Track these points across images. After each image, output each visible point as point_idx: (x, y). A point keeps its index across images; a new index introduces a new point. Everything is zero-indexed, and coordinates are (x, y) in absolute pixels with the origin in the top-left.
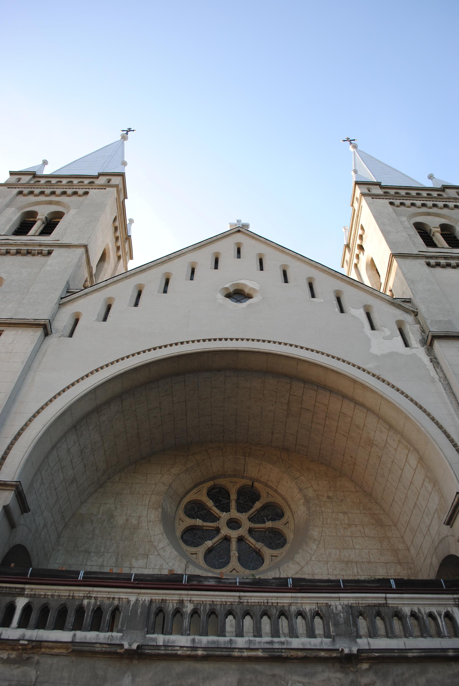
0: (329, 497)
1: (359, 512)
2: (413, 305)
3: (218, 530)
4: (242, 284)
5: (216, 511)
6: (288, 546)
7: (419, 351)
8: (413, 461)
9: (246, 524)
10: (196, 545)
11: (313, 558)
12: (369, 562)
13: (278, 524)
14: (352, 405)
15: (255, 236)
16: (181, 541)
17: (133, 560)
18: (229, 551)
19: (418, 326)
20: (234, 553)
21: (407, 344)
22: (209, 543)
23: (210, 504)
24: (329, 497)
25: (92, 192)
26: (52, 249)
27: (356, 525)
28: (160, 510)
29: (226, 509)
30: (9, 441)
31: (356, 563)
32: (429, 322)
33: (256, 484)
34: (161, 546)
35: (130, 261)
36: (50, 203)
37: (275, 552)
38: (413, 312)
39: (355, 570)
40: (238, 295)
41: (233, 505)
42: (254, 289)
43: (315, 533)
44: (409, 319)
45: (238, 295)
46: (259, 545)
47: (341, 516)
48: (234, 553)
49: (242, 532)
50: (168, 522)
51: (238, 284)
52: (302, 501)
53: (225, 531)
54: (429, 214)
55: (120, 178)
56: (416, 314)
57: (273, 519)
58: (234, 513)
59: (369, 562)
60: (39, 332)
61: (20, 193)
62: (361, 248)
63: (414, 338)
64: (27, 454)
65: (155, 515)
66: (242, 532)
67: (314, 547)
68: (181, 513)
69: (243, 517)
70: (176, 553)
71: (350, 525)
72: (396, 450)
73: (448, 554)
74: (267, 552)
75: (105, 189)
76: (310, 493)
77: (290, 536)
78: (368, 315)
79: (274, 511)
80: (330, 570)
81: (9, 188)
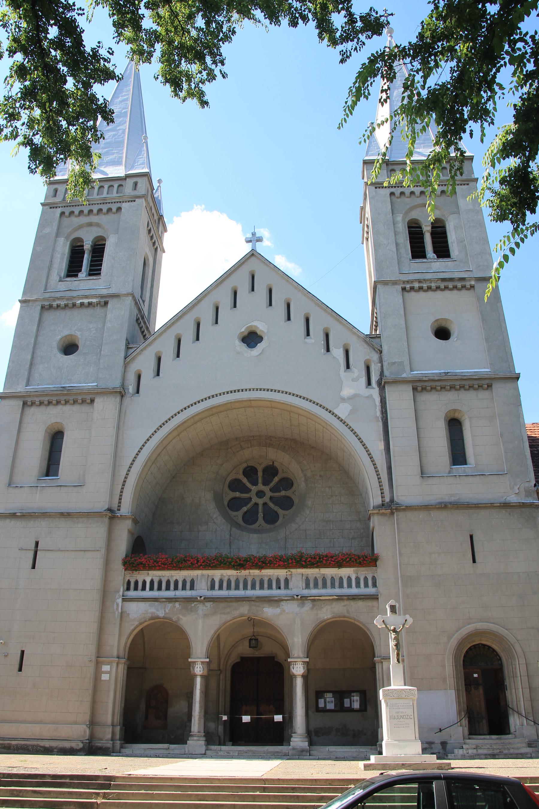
0: (321, 476)
1: (339, 486)
4: (255, 326)
5: (248, 485)
6: (294, 507)
7: (375, 392)
9: (269, 494)
10: (237, 510)
11: (307, 520)
12: (341, 521)
13: (288, 493)
15: (266, 262)
16: (227, 508)
17: (199, 527)
18: (257, 512)
19: (380, 365)
20: (261, 515)
21: (369, 383)
22: (245, 509)
23: (245, 480)
24: (321, 476)
25: (125, 206)
26: (107, 300)
27: (336, 496)
28: (212, 492)
29: (255, 483)
30: (120, 487)
31: (333, 521)
33: (276, 464)
34: (215, 516)
35: (165, 234)
36: (90, 225)
37: (286, 512)
39: (332, 527)
40: (251, 339)
41: (260, 480)
42: (263, 331)
43: (309, 503)
44: (375, 357)
45: (251, 339)
46: (276, 508)
47: (327, 489)
48: (261, 515)
49: (266, 499)
50: (218, 498)
51: (251, 326)
52: (303, 479)
55: (145, 179)
56: (381, 352)
57: (285, 490)
58: (261, 487)
59: (341, 521)
60: (118, 399)
61: (63, 214)
64: (132, 495)
65: (209, 496)
66: (266, 499)
67: (308, 512)
68: (227, 489)
69: (266, 489)
70: (224, 521)
71: (332, 496)
74: (281, 512)
75: (134, 201)
76: (309, 473)
77: (296, 501)
78: (347, 353)
79: (287, 483)
80: (316, 527)
81: (51, 208)
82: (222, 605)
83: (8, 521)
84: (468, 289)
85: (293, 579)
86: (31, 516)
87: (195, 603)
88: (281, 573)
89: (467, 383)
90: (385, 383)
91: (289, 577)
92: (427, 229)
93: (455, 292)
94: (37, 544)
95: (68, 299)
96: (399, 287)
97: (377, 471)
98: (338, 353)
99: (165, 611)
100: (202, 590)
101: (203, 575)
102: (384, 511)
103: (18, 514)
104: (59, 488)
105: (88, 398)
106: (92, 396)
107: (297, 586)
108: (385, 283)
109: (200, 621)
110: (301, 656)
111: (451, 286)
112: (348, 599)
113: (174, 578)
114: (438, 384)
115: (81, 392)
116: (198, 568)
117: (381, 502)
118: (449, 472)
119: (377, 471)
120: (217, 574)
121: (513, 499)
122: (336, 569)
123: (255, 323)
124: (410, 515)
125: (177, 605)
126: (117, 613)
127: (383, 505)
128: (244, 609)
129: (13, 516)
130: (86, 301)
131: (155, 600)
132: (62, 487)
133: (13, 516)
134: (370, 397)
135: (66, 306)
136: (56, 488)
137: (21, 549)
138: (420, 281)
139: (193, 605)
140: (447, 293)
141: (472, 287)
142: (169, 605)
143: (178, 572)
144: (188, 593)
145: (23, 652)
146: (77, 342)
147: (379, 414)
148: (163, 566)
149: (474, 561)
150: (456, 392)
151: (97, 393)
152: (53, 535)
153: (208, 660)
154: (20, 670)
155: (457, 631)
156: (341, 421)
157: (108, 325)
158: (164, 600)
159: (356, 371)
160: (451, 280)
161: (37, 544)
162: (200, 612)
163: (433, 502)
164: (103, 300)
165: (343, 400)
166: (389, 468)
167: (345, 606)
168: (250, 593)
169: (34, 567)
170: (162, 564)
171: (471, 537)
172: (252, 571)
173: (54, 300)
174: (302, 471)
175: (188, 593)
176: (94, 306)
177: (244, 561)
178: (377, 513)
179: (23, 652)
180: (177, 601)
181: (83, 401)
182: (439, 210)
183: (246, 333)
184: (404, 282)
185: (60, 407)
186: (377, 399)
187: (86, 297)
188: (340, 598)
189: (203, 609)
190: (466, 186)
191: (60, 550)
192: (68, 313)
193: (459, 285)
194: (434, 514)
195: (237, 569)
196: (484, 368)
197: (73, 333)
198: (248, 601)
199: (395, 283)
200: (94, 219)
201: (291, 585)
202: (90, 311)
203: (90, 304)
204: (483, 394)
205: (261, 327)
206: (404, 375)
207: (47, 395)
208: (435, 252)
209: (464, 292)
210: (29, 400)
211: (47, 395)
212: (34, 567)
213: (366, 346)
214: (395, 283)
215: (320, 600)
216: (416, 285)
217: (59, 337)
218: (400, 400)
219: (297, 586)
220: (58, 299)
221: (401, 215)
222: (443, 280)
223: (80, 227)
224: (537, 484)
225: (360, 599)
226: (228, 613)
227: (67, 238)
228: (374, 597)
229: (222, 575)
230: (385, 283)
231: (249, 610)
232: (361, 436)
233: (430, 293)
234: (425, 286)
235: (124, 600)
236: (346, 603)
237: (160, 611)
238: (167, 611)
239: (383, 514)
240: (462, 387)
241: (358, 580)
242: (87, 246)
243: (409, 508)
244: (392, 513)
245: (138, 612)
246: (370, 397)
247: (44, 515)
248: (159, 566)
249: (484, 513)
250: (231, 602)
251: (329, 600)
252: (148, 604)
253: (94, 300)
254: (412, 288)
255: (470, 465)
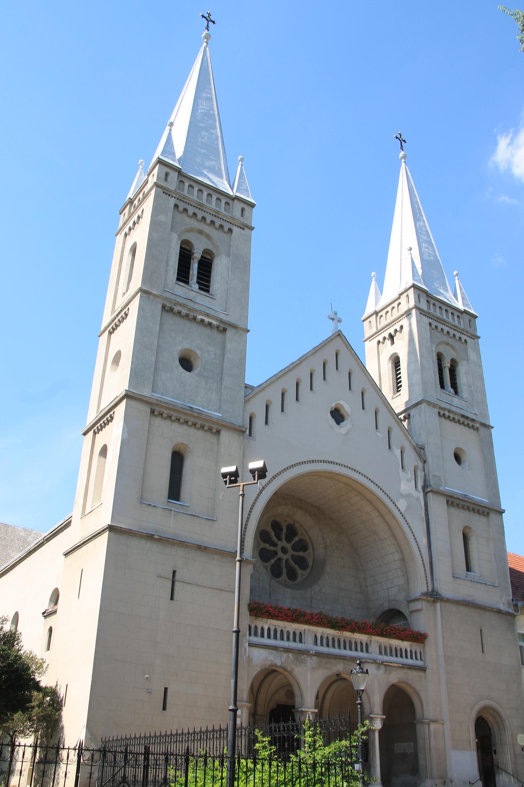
0: (336, 547)
2: (424, 452)
3: (276, 553)
6: (309, 569)
7: (421, 495)
8: (397, 556)
14: (378, 514)
23: (273, 534)
24: (336, 547)
26: (226, 327)
32: (431, 474)
33: (297, 525)
38: (424, 460)
40: (338, 415)
42: (347, 413)
44: (421, 465)
45: (338, 415)
51: (338, 404)
53: (280, 554)
54: (448, 344)
56: (425, 462)
62: (391, 337)
63: (420, 484)
69: (289, 546)
72: (389, 545)
73: (398, 608)
75: (243, 229)
77: (310, 563)
81: (164, 193)
82: (325, 660)
83: (143, 541)
84: (474, 429)
85: (372, 644)
86: (168, 541)
87: (304, 656)
88: (363, 638)
89: (477, 508)
90: (431, 491)
91: (369, 643)
92: (447, 364)
93: (467, 428)
94: (174, 572)
95: (189, 310)
96: (436, 411)
97: (423, 564)
98: (398, 452)
99: (281, 660)
100: (308, 644)
101: (309, 630)
102: (429, 598)
103: (156, 537)
104: (192, 517)
105: (215, 428)
106: (219, 427)
107: (374, 653)
108: (429, 403)
109: (309, 674)
110: (380, 713)
111: (466, 423)
112: (408, 668)
113: (287, 629)
114: (461, 502)
115: (208, 419)
116: (302, 623)
117: (426, 591)
118: (466, 577)
119: (423, 564)
120: (320, 631)
121: (502, 607)
122: (401, 641)
123: (342, 403)
124: (448, 606)
125: (291, 655)
126: (245, 657)
127: (427, 592)
128: (339, 667)
129: (150, 537)
130: (207, 320)
131: (275, 648)
132: (195, 518)
133: (150, 537)
134: (418, 499)
135: (187, 316)
136: (190, 517)
137: (159, 576)
138: (449, 411)
139: (303, 657)
140: (462, 427)
141: (477, 428)
142: (285, 655)
143: (291, 624)
144: (297, 645)
145: (166, 689)
146: (192, 359)
147: (423, 515)
148: (285, 617)
149: (483, 652)
150: (469, 512)
151: (224, 426)
152: (192, 568)
153: (317, 710)
154: (164, 708)
155: (475, 704)
156: (401, 513)
157: (228, 356)
158: (282, 649)
159: (409, 473)
160: (467, 418)
161: (174, 572)
162: (309, 665)
163: (460, 599)
164: (222, 326)
165: (402, 496)
166: (431, 563)
167: (405, 673)
168: (343, 652)
169: (172, 598)
170: (285, 615)
171: (481, 630)
172: (345, 633)
173: (175, 304)
174: (323, 539)
175: (297, 645)
176: (212, 328)
177: (346, 623)
178: (425, 599)
179: (166, 689)
180: (291, 652)
181: (210, 430)
182: (456, 352)
183: (342, 412)
184: (440, 408)
185: (185, 427)
186: (423, 503)
187: (208, 315)
188: (404, 666)
189: (311, 662)
190: (472, 340)
191: (197, 585)
192: (188, 324)
193: (471, 424)
194: (461, 608)
195: (340, 630)
196: (484, 498)
197: (193, 349)
198: (343, 659)
199: (435, 406)
200: (207, 229)
201: (370, 650)
202: (207, 331)
203: (210, 324)
204: (483, 519)
205: (346, 408)
206: (441, 488)
207: (169, 409)
208: (452, 387)
209: (472, 430)
210: (157, 409)
211: (169, 409)
212: (172, 598)
213: (415, 453)
214: (435, 406)
215: (390, 666)
216: (447, 414)
217: (180, 348)
218: (438, 507)
219: (374, 653)
220: (180, 305)
221: (435, 346)
222: (463, 416)
223: (191, 230)
224: (514, 599)
225: (414, 669)
226: (329, 668)
227: (179, 236)
228: (423, 669)
229: (322, 633)
230: (429, 403)
231: (344, 668)
232: (413, 530)
233: (453, 424)
234: (452, 416)
235: (250, 645)
236: (406, 671)
237: (277, 659)
238: (283, 660)
239: (428, 601)
240: (473, 510)
241: (411, 651)
242: (197, 255)
243: (448, 601)
244: (434, 602)
245: (259, 658)
246: (418, 499)
247: (182, 544)
248: (281, 617)
249: (487, 614)
250: (331, 658)
251: (395, 666)
252: (267, 651)
253: (214, 322)
254: (444, 415)
255: (474, 573)
